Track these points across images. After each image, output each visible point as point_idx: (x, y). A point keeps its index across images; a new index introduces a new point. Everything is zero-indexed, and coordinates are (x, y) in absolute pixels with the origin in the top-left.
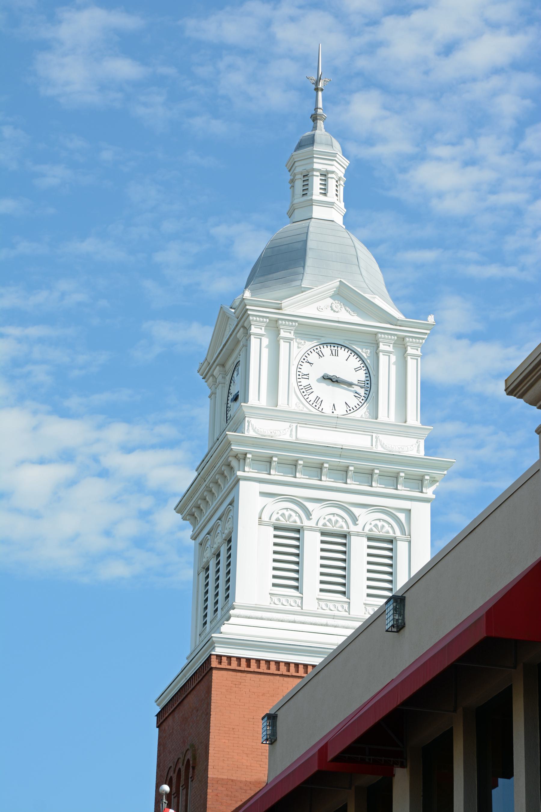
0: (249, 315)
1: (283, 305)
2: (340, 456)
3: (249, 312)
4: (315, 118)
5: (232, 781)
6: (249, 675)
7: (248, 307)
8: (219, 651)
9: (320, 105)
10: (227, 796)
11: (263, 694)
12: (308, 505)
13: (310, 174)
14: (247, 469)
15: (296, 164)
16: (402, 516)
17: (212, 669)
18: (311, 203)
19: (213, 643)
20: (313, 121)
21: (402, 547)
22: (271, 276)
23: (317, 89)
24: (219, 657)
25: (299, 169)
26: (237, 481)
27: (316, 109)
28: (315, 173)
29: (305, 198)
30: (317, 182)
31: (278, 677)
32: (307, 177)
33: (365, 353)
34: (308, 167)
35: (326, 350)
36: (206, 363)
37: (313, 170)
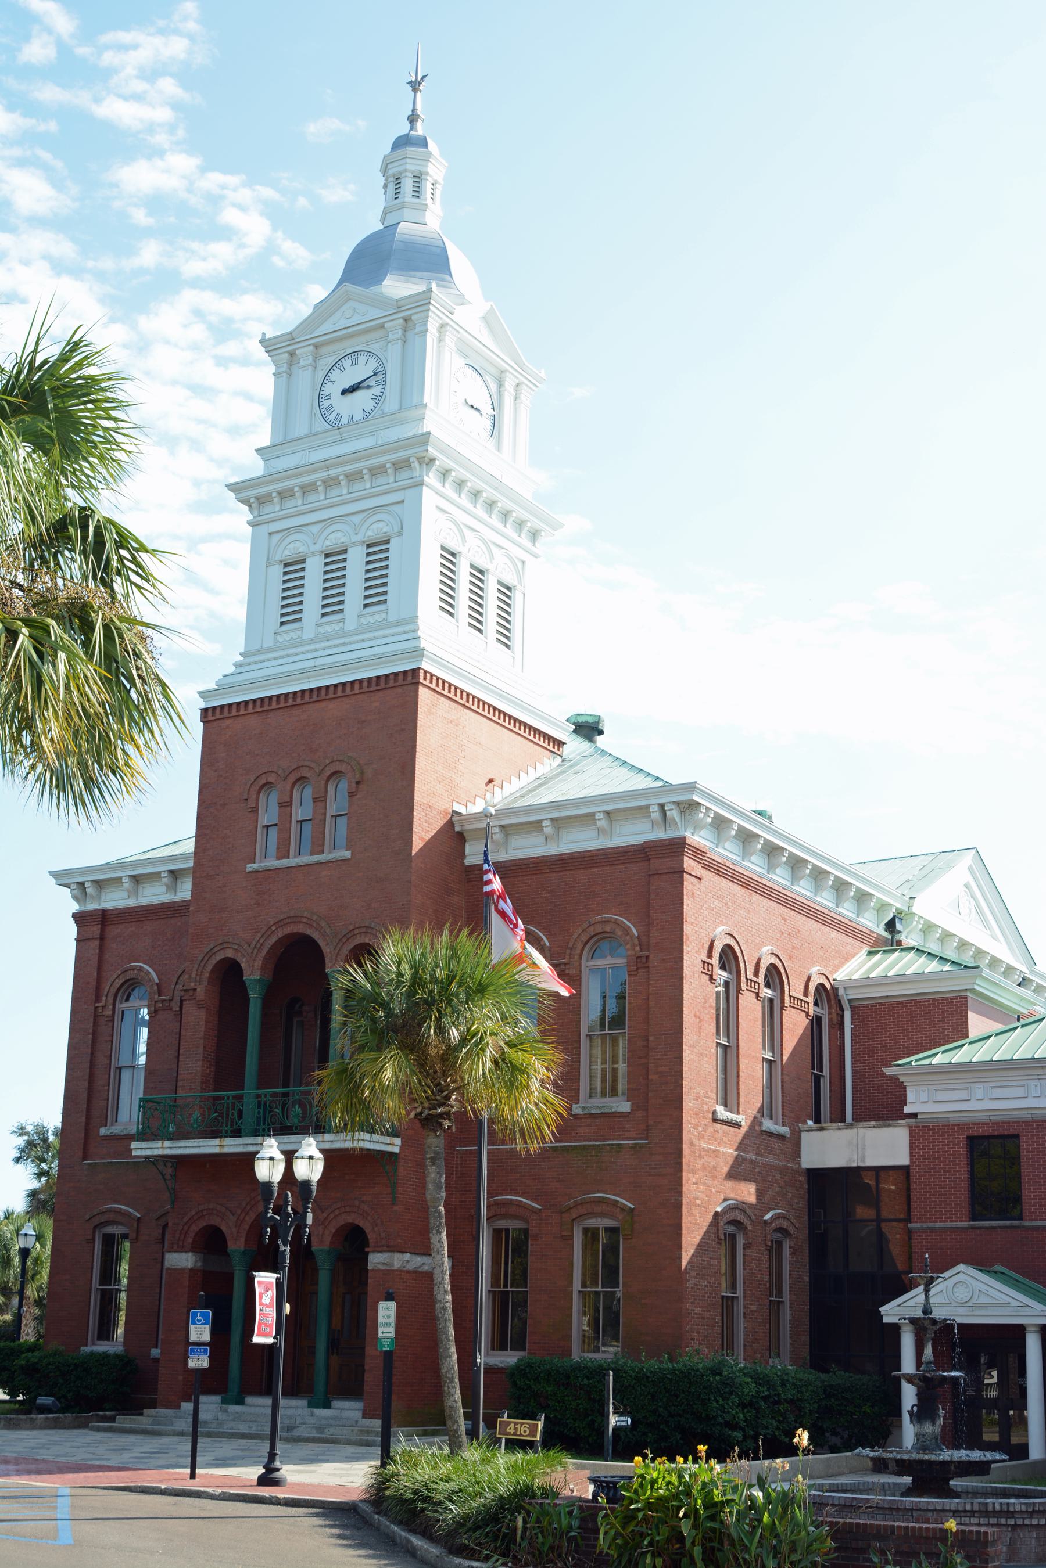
0: (429, 310)
1: (456, 312)
2: (496, 489)
3: (431, 307)
4: (413, 119)
5: (430, 807)
6: (443, 699)
7: (432, 301)
8: (425, 665)
9: (419, 106)
10: (426, 821)
11: (451, 722)
12: (465, 531)
13: (424, 177)
14: (431, 475)
15: (408, 160)
16: (519, 564)
17: (418, 683)
18: (424, 208)
19: (423, 655)
20: (411, 122)
21: (517, 597)
22: (412, 273)
23: (415, 90)
24: (426, 672)
25: (411, 166)
26: (421, 484)
27: (414, 110)
28: (428, 178)
29: (416, 200)
30: (428, 187)
31: (460, 707)
32: (418, 178)
33: (494, 387)
34: (422, 169)
35: (470, 372)
36: (289, 337)
37: (427, 174)
